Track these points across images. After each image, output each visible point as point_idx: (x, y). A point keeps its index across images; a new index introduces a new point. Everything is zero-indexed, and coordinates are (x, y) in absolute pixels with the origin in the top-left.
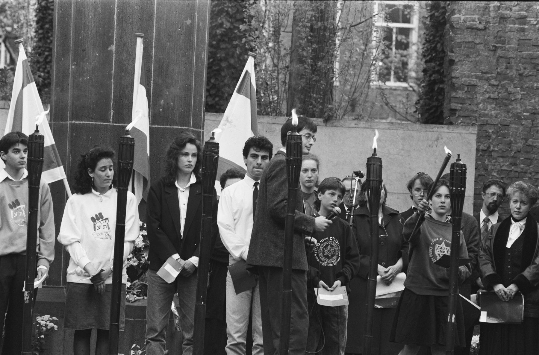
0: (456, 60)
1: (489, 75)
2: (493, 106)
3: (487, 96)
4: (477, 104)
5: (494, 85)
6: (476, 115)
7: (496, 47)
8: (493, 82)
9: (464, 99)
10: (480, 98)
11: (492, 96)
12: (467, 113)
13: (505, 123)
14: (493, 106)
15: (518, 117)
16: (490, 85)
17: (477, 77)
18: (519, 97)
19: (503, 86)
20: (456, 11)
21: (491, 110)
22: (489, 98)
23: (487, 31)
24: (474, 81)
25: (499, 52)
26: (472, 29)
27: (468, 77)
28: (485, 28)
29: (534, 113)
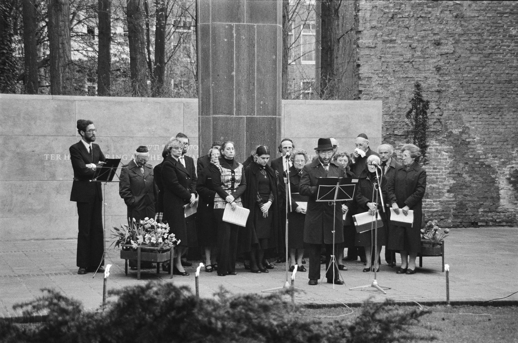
0: (361, 64)
1: (378, 72)
2: (381, 88)
3: (377, 83)
4: (373, 87)
5: (381, 77)
6: (372, 93)
7: (381, 56)
8: (381, 75)
9: (365, 85)
10: (374, 84)
11: (380, 82)
12: (367, 92)
13: (387, 97)
14: (381, 88)
15: (393, 93)
16: (379, 77)
17: (372, 73)
18: (393, 82)
19: (385, 77)
20: (360, 39)
21: (379, 90)
22: (378, 84)
23: (376, 48)
24: (371, 75)
25: (383, 59)
26: (369, 47)
27: (368, 73)
28: (375, 47)
29: (401, 91)
